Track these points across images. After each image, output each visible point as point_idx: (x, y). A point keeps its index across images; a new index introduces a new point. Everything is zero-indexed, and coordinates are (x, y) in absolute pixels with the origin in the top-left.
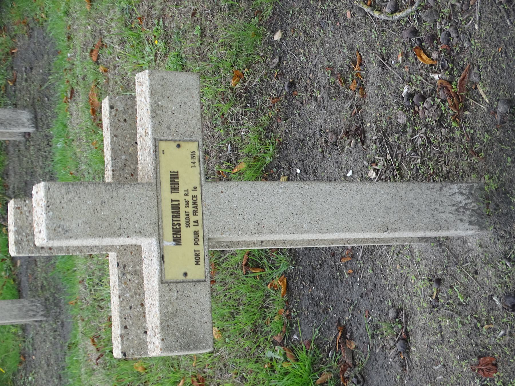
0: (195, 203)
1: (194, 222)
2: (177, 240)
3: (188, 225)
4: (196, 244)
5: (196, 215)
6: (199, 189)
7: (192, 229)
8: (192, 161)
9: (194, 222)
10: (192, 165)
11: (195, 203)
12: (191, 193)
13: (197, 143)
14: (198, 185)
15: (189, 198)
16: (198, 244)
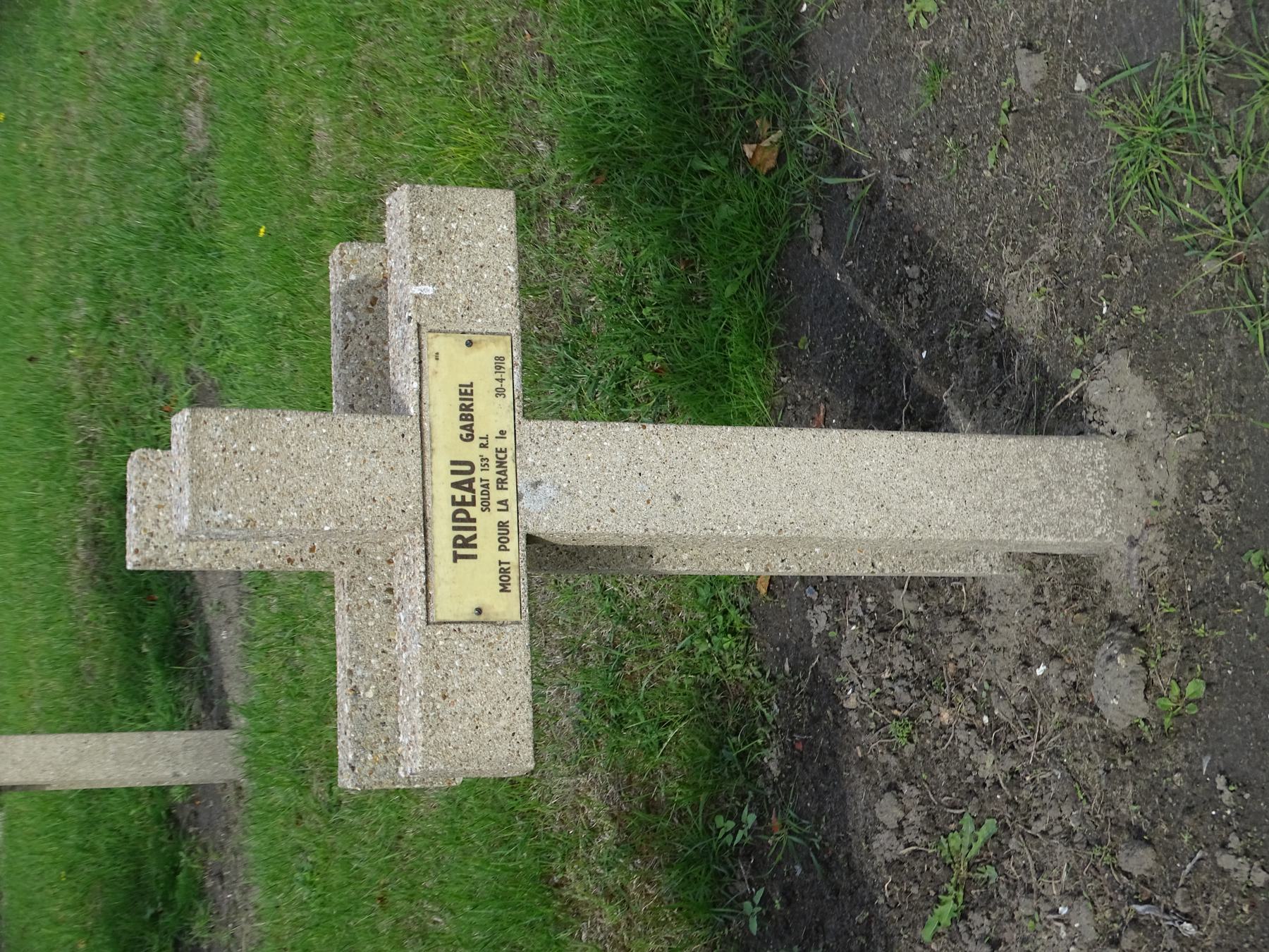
0: (501, 463)
1: (500, 502)
2: (464, 545)
3: (486, 507)
4: (503, 547)
5: (502, 488)
6: (510, 436)
7: (496, 516)
8: (498, 376)
9: (500, 502)
10: (499, 385)
11: (501, 463)
12: (494, 444)
13: (508, 338)
14: (507, 424)
15: (489, 453)
16: (507, 550)
